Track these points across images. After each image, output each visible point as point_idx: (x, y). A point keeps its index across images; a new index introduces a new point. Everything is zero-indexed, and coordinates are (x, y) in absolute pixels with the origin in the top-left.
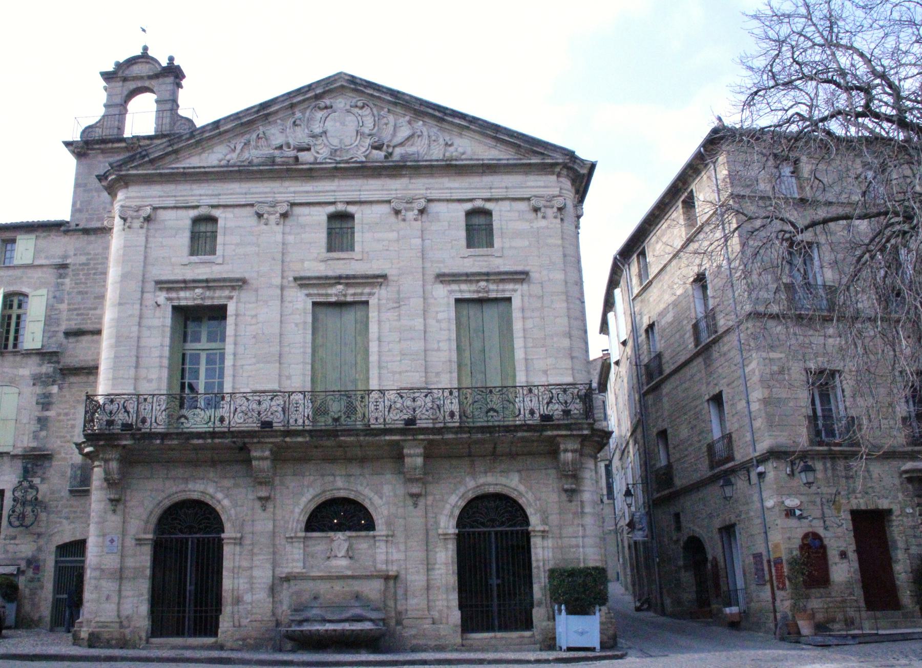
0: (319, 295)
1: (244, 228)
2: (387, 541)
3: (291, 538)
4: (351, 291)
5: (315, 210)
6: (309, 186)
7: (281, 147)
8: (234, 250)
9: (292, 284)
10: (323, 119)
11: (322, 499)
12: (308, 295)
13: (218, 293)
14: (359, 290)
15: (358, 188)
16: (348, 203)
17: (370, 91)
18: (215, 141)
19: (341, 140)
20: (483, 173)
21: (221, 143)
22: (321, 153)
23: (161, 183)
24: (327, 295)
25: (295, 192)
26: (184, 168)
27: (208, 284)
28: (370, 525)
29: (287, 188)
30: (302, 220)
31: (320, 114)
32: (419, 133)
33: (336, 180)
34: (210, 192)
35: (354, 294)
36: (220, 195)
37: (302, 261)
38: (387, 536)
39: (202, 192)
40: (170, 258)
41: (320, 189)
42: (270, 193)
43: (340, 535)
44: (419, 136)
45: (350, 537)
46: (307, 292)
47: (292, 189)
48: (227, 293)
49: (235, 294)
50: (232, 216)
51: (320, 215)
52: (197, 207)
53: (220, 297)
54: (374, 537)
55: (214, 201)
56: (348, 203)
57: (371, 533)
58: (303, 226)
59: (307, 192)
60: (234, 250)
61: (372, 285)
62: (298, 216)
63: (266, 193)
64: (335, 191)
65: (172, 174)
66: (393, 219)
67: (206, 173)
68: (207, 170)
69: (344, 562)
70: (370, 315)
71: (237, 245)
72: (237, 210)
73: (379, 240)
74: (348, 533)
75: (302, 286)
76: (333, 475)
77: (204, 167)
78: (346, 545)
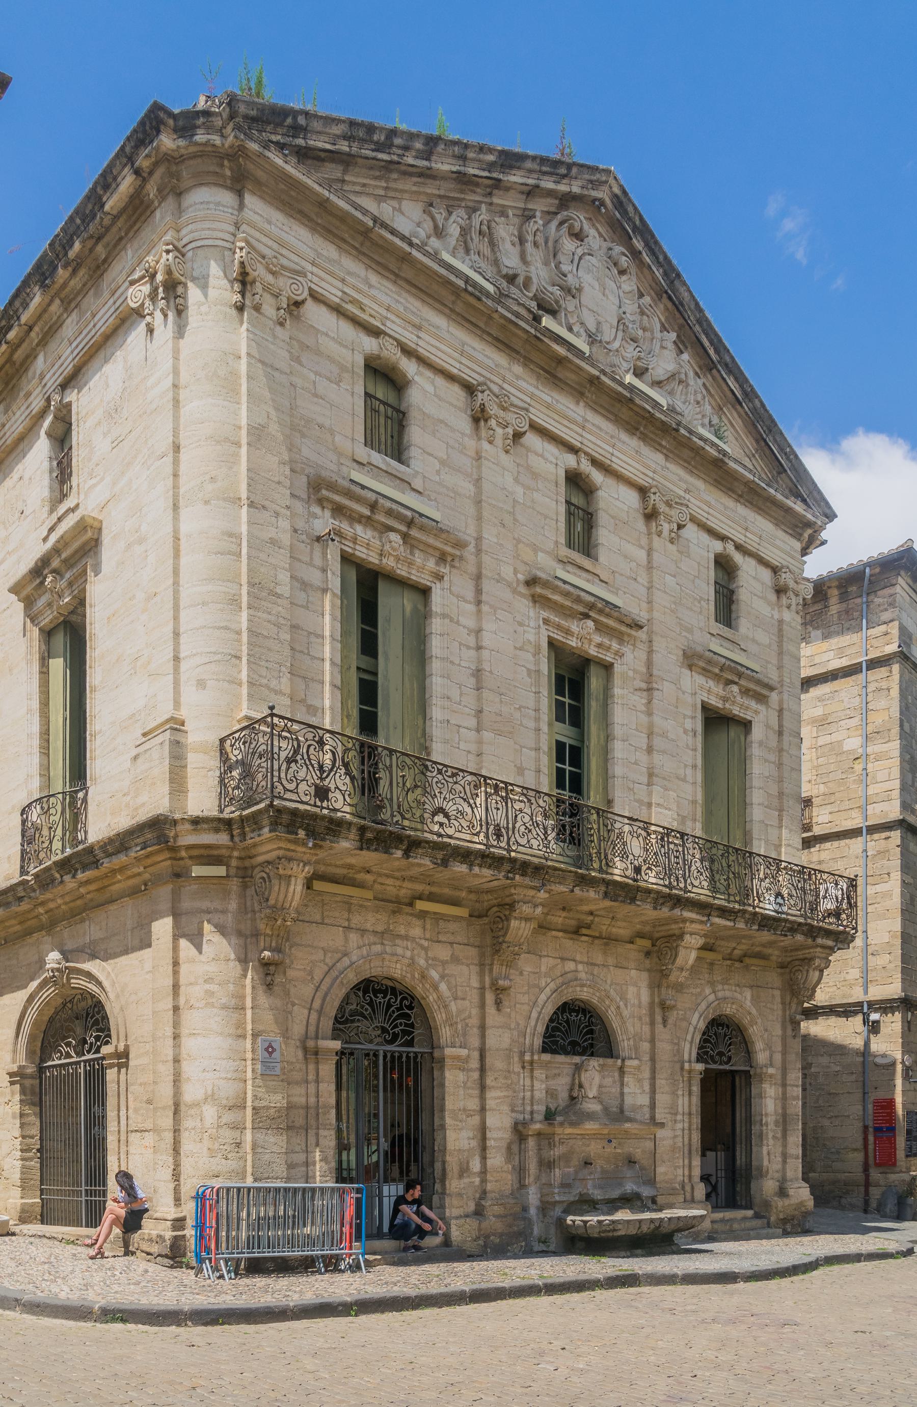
0: (559, 627)
1: (453, 430)
4: (597, 639)
5: (551, 449)
6: (547, 395)
7: (511, 279)
9: (523, 589)
10: (576, 258)
12: (546, 621)
14: (606, 641)
17: (638, 244)
18: (408, 184)
20: (739, 498)
21: (415, 196)
23: (314, 226)
24: (568, 632)
29: (518, 377)
30: (534, 460)
31: (569, 245)
32: (683, 376)
35: (599, 646)
36: (419, 328)
44: (680, 382)
46: (545, 614)
49: (445, 570)
51: (553, 463)
55: (409, 337)
56: (595, 462)
58: (535, 476)
60: (438, 472)
61: (620, 637)
62: (528, 450)
65: (344, 218)
66: (641, 524)
67: (406, 258)
70: (617, 691)
72: (440, 381)
73: (626, 557)
75: (536, 600)
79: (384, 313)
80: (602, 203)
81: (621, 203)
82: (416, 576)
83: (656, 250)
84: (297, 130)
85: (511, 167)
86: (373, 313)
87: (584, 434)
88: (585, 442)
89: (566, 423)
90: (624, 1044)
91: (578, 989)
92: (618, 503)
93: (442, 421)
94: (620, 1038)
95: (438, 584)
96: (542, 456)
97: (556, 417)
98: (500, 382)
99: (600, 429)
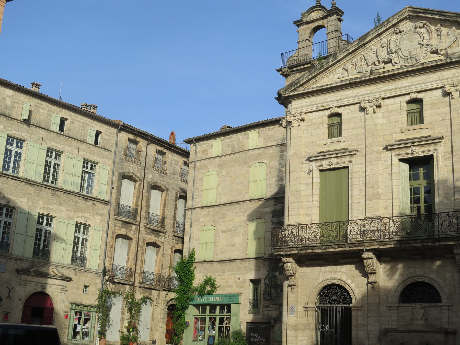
2: (448, 309)
3: (390, 307)
8: (351, 133)
11: (409, 282)
12: (396, 155)
13: (344, 159)
15: (423, 82)
16: (418, 92)
19: (410, 52)
22: (399, 64)
25: (384, 91)
26: (319, 87)
27: (338, 154)
28: (439, 300)
33: (409, 78)
34: (335, 99)
36: (341, 100)
37: (391, 134)
38: (449, 306)
39: (331, 99)
40: (316, 142)
41: (399, 86)
42: (369, 94)
43: (418, 305)
45: (425, 307)
47: (383, 89)
48: (348, 159)
50: (349, 111)
52: (329, 109)
53: (345, 162)
54: (440, 306)
56: (418, 92)
57: (439, 304)
59: (392, 90)
63: (367, 94)
64: (408, 86)
68: (332, 86)
69: (421, 322)
71: (353, 129)
74: (424, 304)
76: (414, 268)
77: (330, 85)
78: (422, 312)
79: (329, 103)
80: (409, 15)
81: (414, 11)
82: (343, 165)
83: (433, 12)
84: (297, 84)
85: (365, 39)
86: (326, 106)
87: (409, 88)
88: (411, 90)
89: (401, 89)
90: (444, 297)
91: (416, 278)
92: (433, 98)
93: (352, 118)
94: (441, 295)
95: (351, 164)
96: (395, 104)
97: (396, 90)
98: (371, 95)
99: (419, 81)
